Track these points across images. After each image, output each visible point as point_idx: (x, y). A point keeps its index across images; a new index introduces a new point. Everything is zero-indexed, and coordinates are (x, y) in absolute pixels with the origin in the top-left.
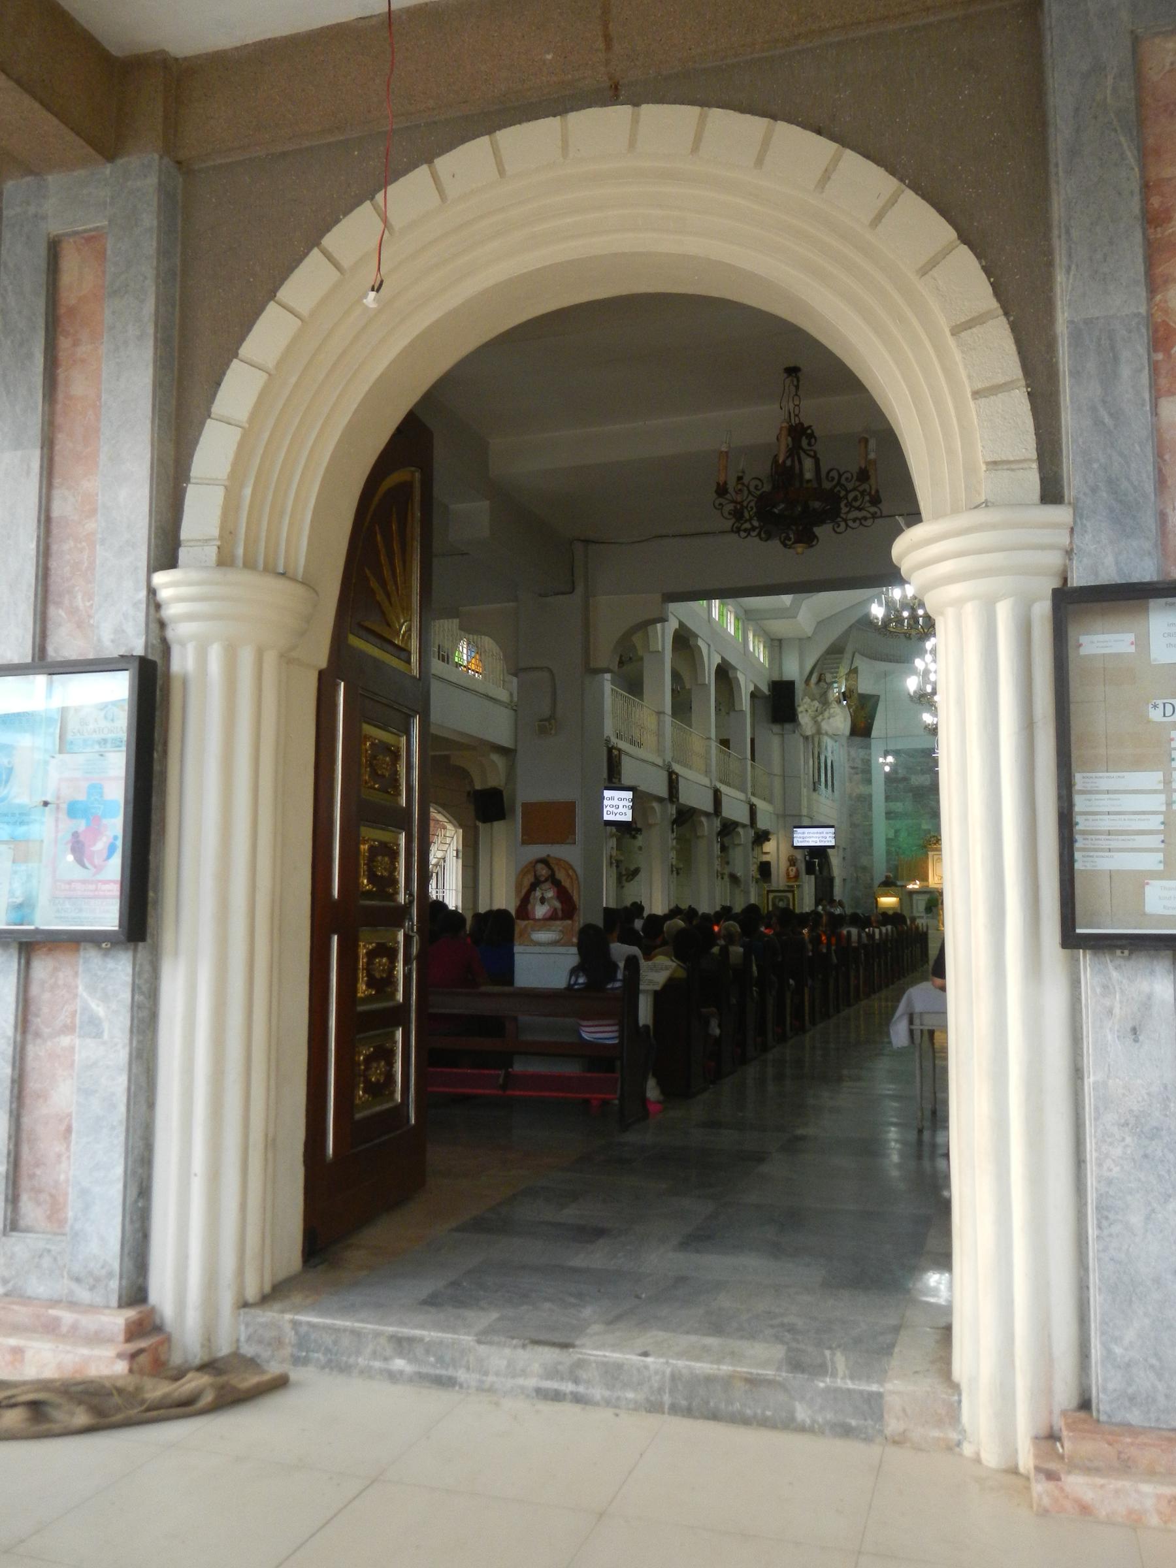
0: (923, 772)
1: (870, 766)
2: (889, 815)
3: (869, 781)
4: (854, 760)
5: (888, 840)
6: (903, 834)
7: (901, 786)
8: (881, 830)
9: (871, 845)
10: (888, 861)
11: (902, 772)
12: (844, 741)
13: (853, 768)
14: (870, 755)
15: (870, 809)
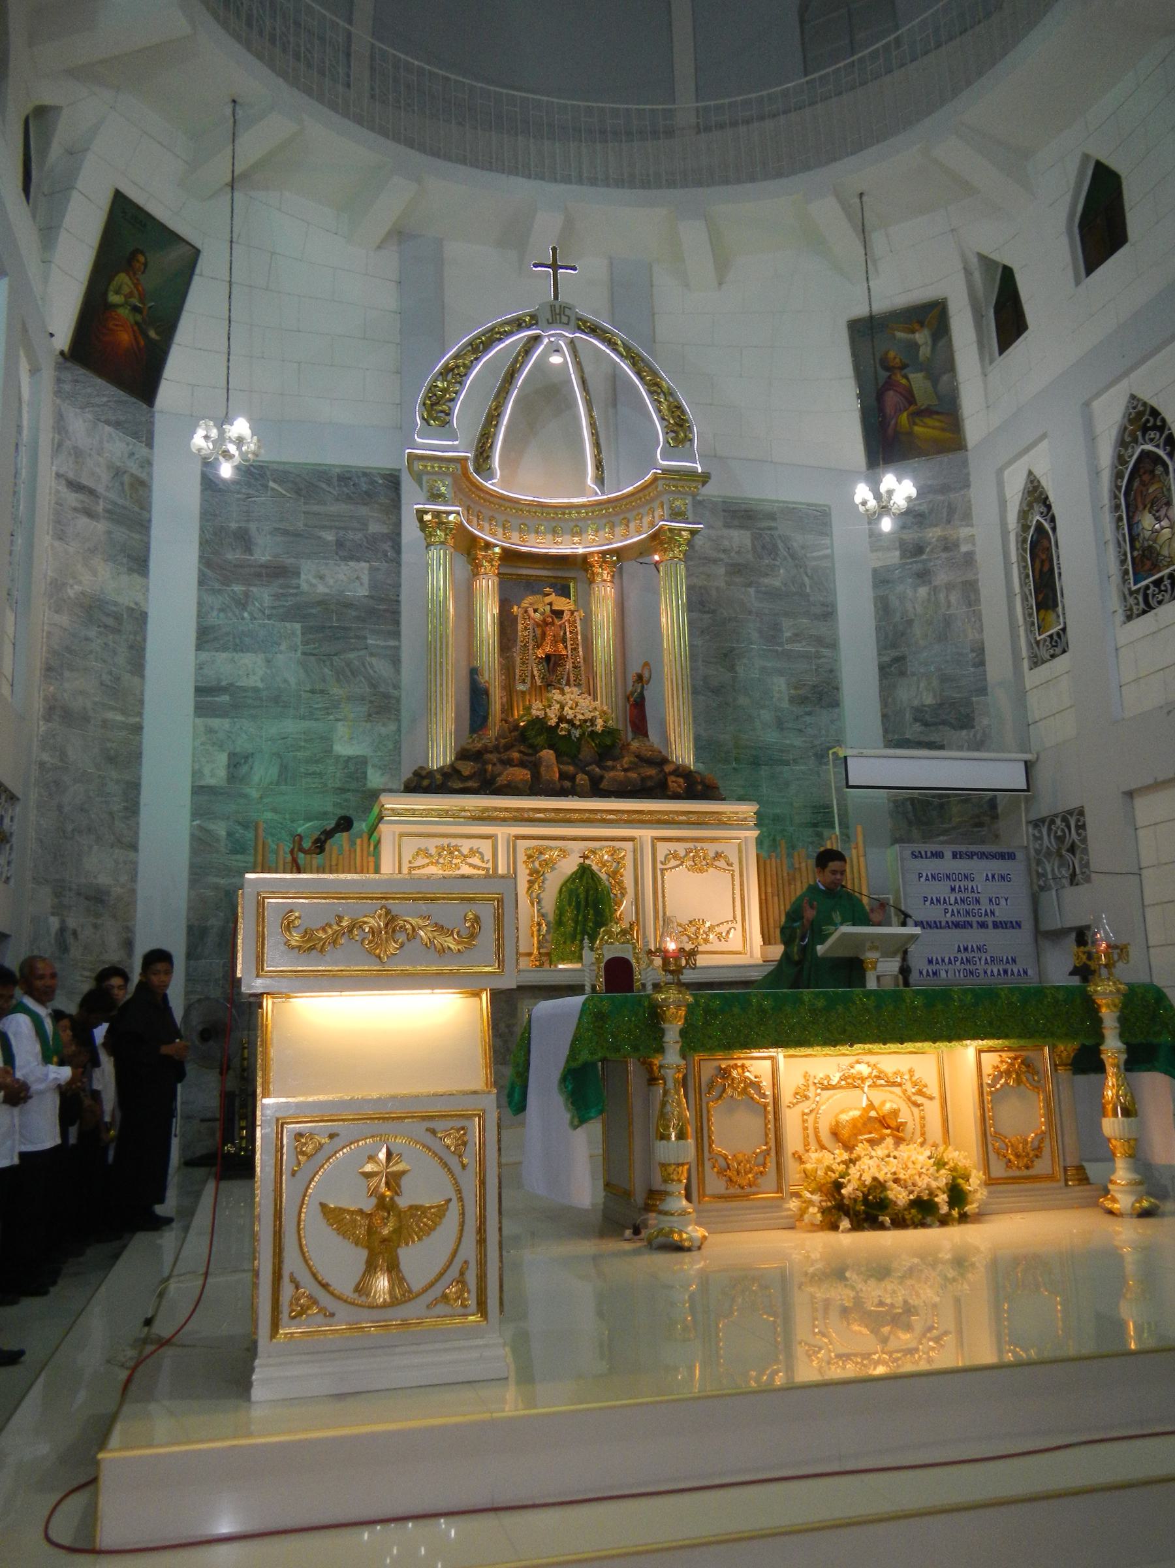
0: (346, 551)
1: (145, 505)
2: (210, 697)
3: (139, 562)
4: (78, 454)
5: (198, 790)
6: (262, 772)
7: (264, 595)
8: (173, 754)
9: (132, 809)
10: (197, 873)
11: (265, 551)
12: (48, 374)
13: (75, 486)
14: (148, 463)
15: (138, 665)
